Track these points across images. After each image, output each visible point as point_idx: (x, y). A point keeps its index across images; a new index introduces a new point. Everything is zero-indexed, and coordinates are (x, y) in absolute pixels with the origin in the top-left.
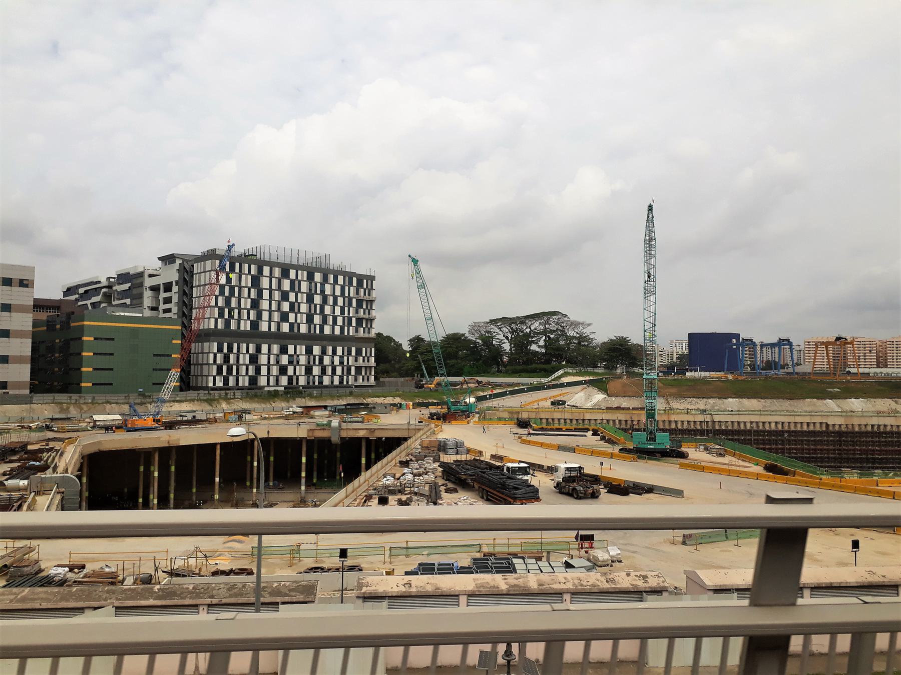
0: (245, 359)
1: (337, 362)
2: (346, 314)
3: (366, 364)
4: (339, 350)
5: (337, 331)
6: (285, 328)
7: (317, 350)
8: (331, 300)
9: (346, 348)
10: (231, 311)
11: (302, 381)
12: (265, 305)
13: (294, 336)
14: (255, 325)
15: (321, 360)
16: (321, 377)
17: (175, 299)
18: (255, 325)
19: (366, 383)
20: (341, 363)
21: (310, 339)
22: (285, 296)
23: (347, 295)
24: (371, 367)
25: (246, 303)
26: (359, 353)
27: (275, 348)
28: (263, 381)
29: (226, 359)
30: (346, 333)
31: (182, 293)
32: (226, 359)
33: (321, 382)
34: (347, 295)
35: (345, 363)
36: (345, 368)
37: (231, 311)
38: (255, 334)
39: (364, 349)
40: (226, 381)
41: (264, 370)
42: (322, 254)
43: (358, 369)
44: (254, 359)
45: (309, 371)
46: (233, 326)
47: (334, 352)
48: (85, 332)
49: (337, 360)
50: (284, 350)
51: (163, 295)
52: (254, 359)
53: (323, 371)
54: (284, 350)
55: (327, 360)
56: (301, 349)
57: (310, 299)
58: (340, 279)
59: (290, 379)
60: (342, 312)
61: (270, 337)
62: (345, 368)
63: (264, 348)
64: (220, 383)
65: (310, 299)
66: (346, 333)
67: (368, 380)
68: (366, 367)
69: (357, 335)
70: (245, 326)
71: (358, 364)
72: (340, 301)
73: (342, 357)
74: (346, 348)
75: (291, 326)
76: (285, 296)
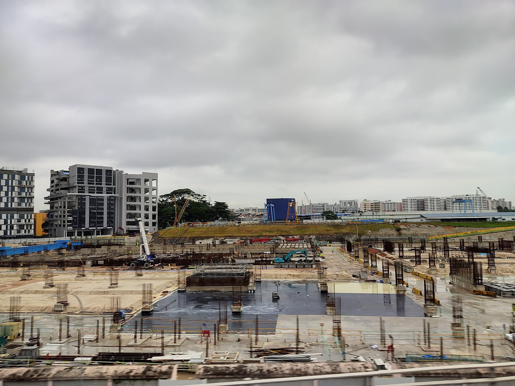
2: (10, 195)
9: (9, 215)
19: (27, 234)
23: (10, 184)
24: (31, 225)
26: (22, 217)
30: (9, 206)
34: (10, 184)
35: (9, 223)
36: (9, 226)
39: (26, 215)
43: (21, 227)
62: (9, 226)
66: (9, 206)
67: (29, 232)
68: (27, 225)
69: (19, 207)
71: (20, 223)
74: (9, 215)
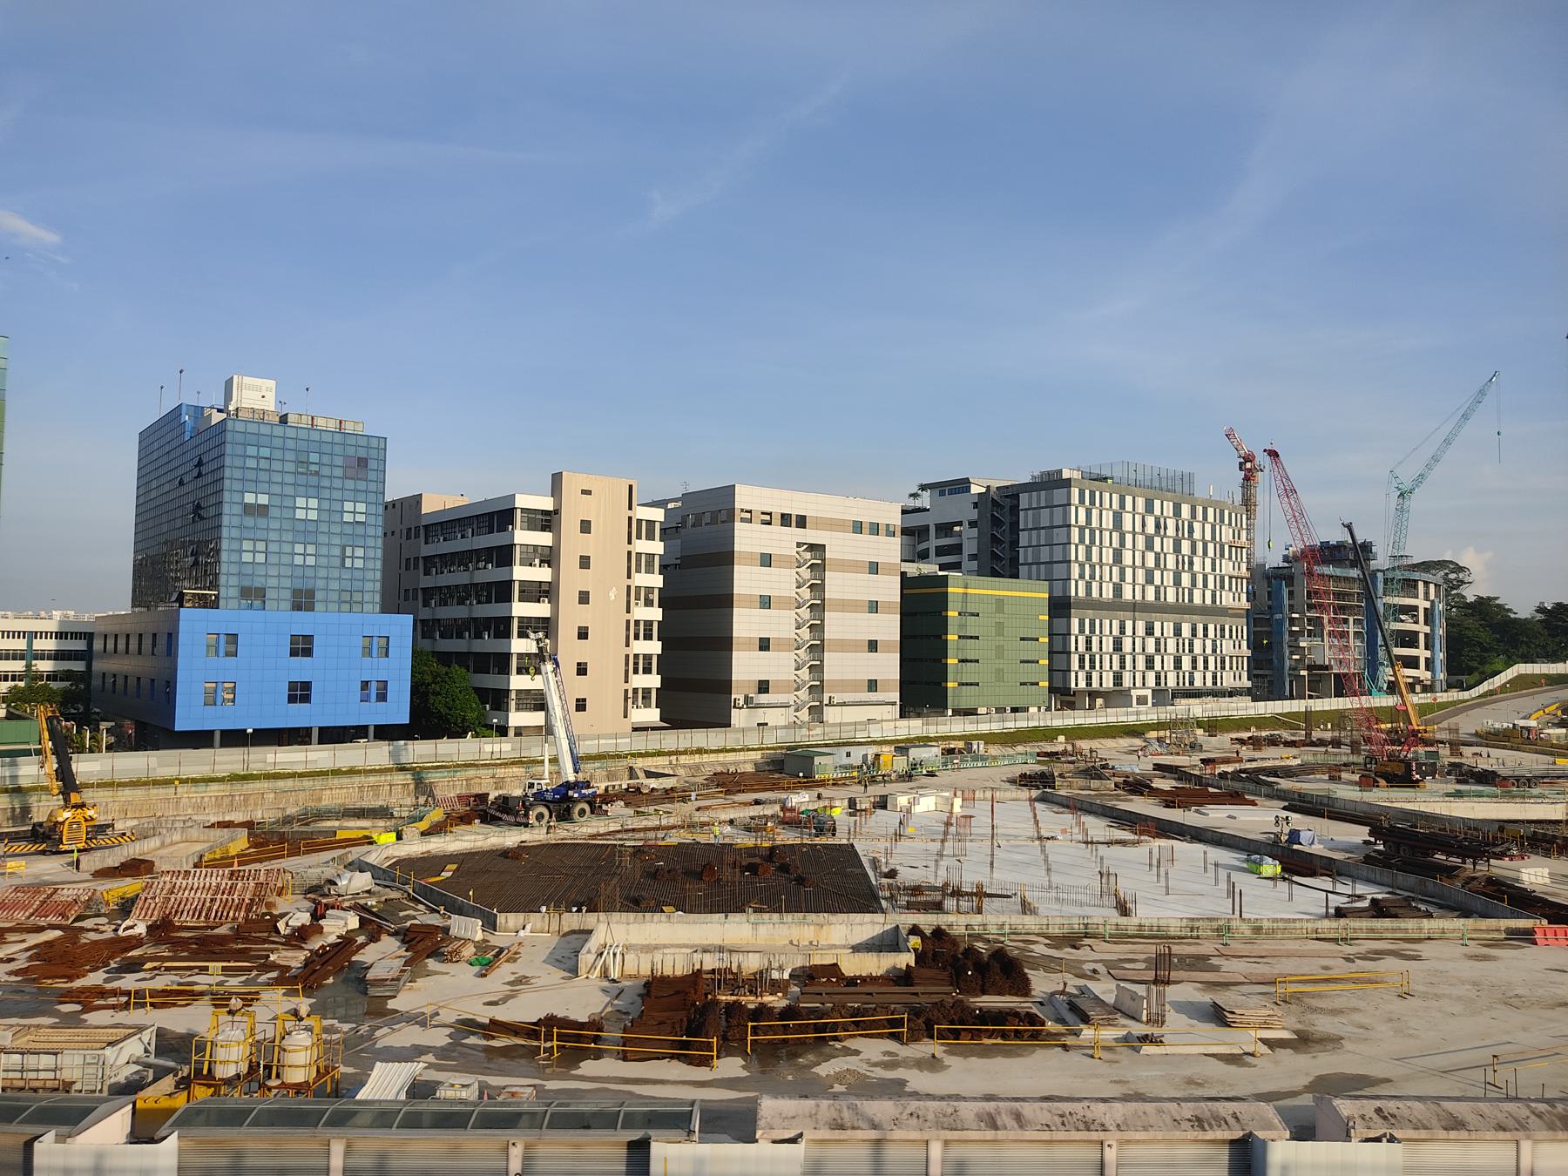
0: (1108, 645)
1: (1209, 650)
3: (1236, 652)
4: (1211, 627)
5: (1208, 601)
6: (1151, 597)
7: (1186, 630)
8: (1200, 546)
10: (1092, 567)
11: (1172, 683)
12: (1127, 558)
13: (1160, 608)
14: (1118, 590)
15: (1191, 645)
16: (1191, 674)
17: (970, 547)
18: (1118, 590)
19: (1238, 684)
20: (1214, 651)
21: (1183, 609)
22: (1149, 545)
25: (1108, 556)
27: (1141, 626)
28: (1127, 681)
29: (1089, 642)
31: (988, 539)
32: (1089, 642)
33: (1192, 683)
37: (1092, 567)
38: (1118, 605)
40: (1089, 678)
41: (1128, 659)
42: (1187, 471)
44: (1118, 645)
45: (1178, 663)
46: (1095, 594)
47: (1206, 635)
48: (950, 605)
49: (1209, 643)
50: (1150, 631)
51: (933, 542)
52: (1118, 645)
53: (1194, 661)
54: (1150, 631)
55: (1197, 649)
56: (1169, 628)
57: (1177, 549)
58: (1210, 511)
59: (1158, 677)
60: (1214, 569)
61: (1135, 607)
63: (1129, 624)
64: (1082, 684)
65: (1177, 549)
70: (1108, 593)
72: (1211, 546)
73: (1214, 642)
75: (1157, 589)
76: (1149, 545)
